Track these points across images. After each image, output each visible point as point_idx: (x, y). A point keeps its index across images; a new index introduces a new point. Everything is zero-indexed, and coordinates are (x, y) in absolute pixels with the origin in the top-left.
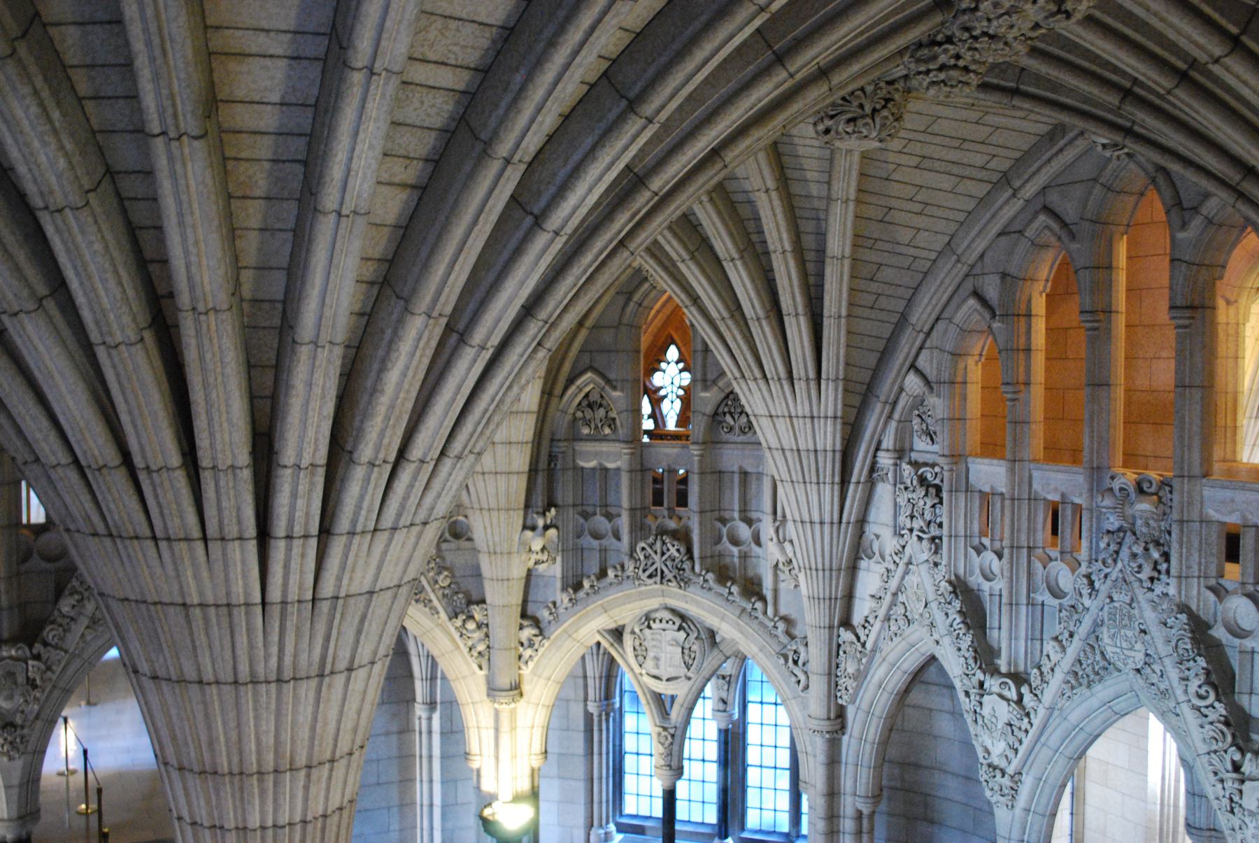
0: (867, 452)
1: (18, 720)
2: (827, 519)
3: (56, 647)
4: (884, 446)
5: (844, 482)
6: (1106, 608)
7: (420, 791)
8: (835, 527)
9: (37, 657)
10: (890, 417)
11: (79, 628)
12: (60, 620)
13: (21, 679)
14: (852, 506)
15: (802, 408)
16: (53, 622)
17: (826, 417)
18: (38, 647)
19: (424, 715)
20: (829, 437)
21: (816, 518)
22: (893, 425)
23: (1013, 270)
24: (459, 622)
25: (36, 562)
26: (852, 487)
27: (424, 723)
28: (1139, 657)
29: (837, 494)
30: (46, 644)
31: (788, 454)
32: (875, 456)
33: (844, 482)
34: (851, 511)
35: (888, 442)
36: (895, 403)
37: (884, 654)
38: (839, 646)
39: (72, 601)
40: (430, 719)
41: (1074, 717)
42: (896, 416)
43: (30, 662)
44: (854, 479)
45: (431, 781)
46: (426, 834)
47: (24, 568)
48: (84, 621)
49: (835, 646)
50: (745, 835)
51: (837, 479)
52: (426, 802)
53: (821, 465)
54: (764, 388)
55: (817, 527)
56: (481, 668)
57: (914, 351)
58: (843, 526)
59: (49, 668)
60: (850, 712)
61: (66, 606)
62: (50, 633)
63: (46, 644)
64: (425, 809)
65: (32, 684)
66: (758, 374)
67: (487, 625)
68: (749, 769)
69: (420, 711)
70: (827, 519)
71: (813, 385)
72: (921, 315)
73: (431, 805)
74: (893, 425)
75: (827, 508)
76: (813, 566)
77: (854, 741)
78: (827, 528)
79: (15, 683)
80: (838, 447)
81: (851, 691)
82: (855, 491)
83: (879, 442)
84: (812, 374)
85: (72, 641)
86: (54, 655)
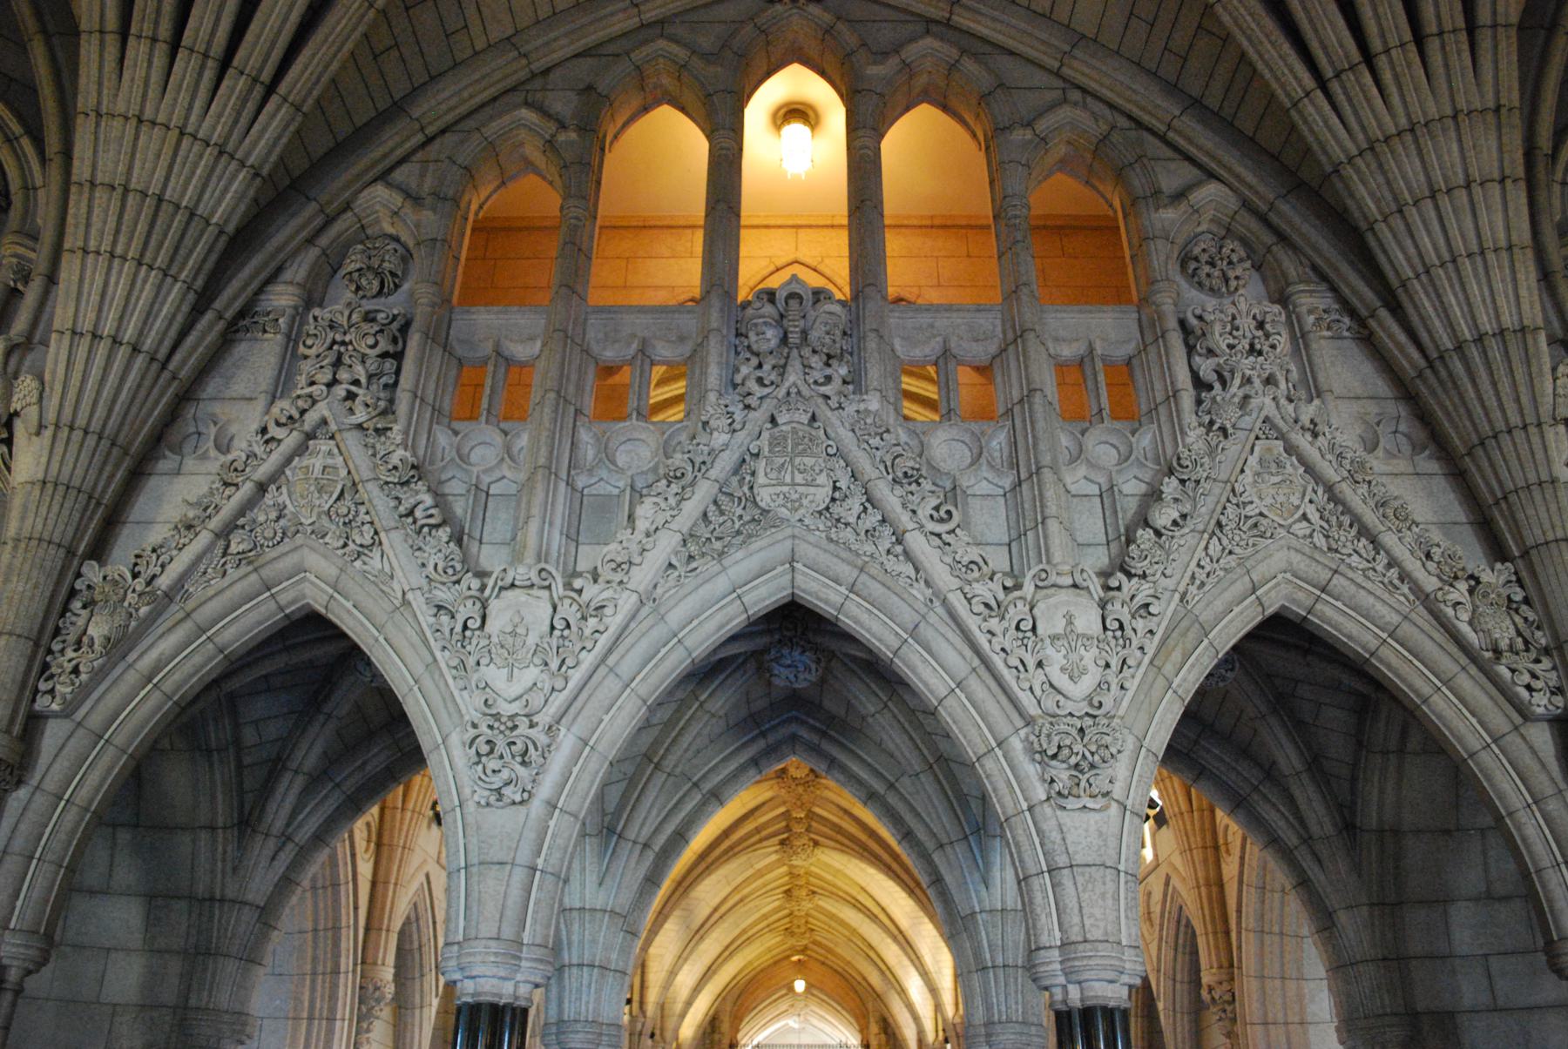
0: (252, 277)
2: (148, 344)
4: (287, 275)
5: (197, 311)
6: (766, 435)
8: (155, 366)
10: (310, 241)
14: (194, 348)
15: (215, 126)
17: (242, 164)
20: (226, 200)
21: (129, 334)
22: (313, 253)
23: (602, 87)
26: (209, 316)
28: (822, 494)
29: (185, 308)
31: (131, 200)
32: (260, 290)
33: (197, 311)
34: (186, 361)
35: (298, 271)
36: (329, 221)
37: (190, 605)
38: (73, 593)
41: (675, 617)
42: (324, 241)
44: (218, 305)
49: (64, 591)
51: (199, 283)
53: (188, 241)
54: (159, 61)
55: (122, 353)
57: (399, 153)
58: (166, 375)
60: (52, 735)
66: (165, 30)
70: (148, 344)
71: (258, 91)
72: (436, 106)
74: (313, 253)
75: (158, 324)
76: (81, 421)
77: (40, 801)
78: (140, 361)
80: (231, 228)
81: (84, 677)
82: (211, 327)
83: (279, 270)
84: (266, 76)
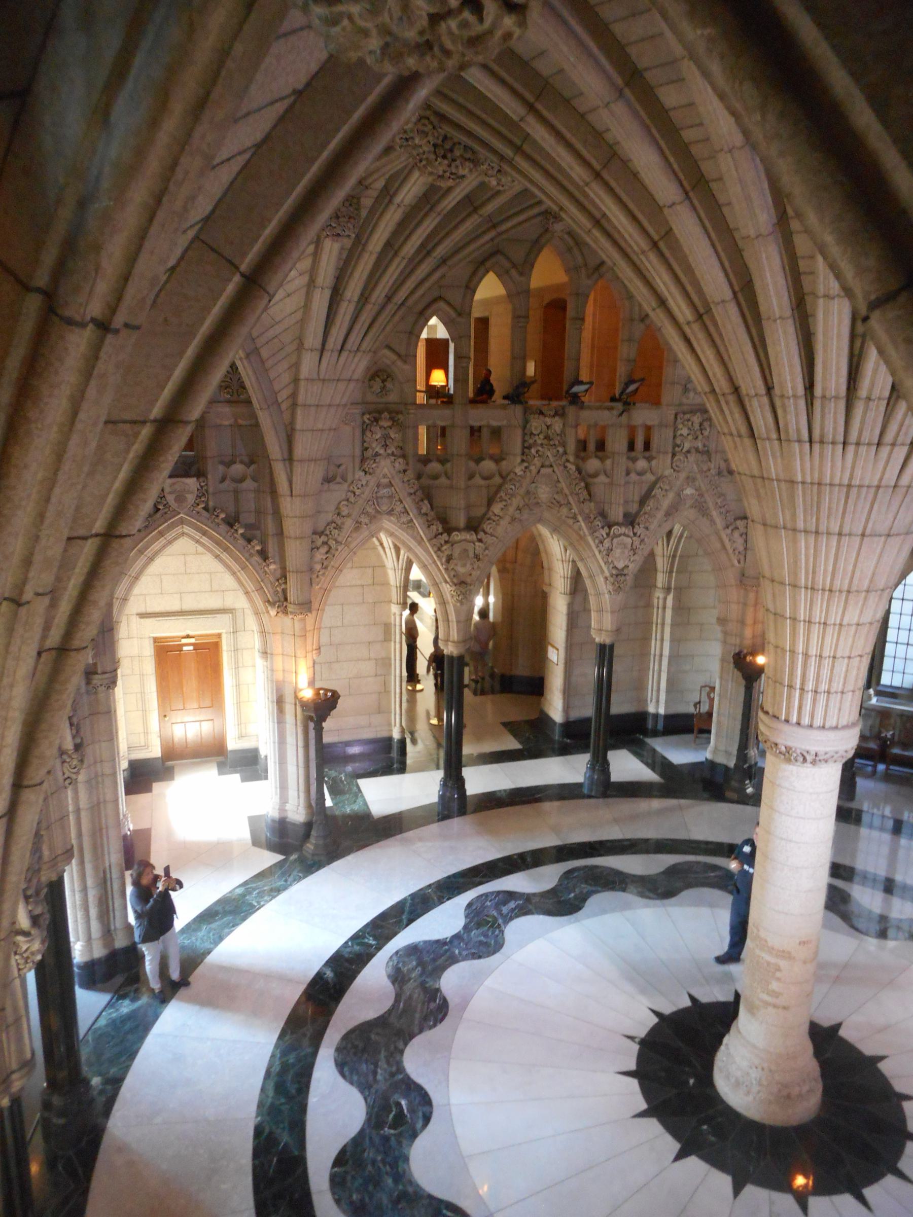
1: (468, 580)
3: (492, 535)
7: (654, 646)
9: (480, 540)
11: (504, 523)
12: (493, 517)
13: (471, 554)
16: (489, 519)
18: (481, 535)
19: (661, 596)
24: (729, 531)
25: (478, 480)
27: (661, 602)
30: (486, 533)
39: (501, 505)
40: (665, 599)
43: (477, 544)
45: (662, 640)
46: (656, 674)
47: (470, 483)
48: (507, 519)
50: (880, 688)
52: (658, 653)
56: (739, 562)
59: (486, 549)
61: (496, 508)
62: (486, 526)
63: (486, 533)
64: (657, 658)
65: (477, 557)
67: (746, 534)
68: (887, 645)
69: (659, 594)
73: (661, 655)
79: (468, 556)
85: (500, 531)
86: (488, 540)
